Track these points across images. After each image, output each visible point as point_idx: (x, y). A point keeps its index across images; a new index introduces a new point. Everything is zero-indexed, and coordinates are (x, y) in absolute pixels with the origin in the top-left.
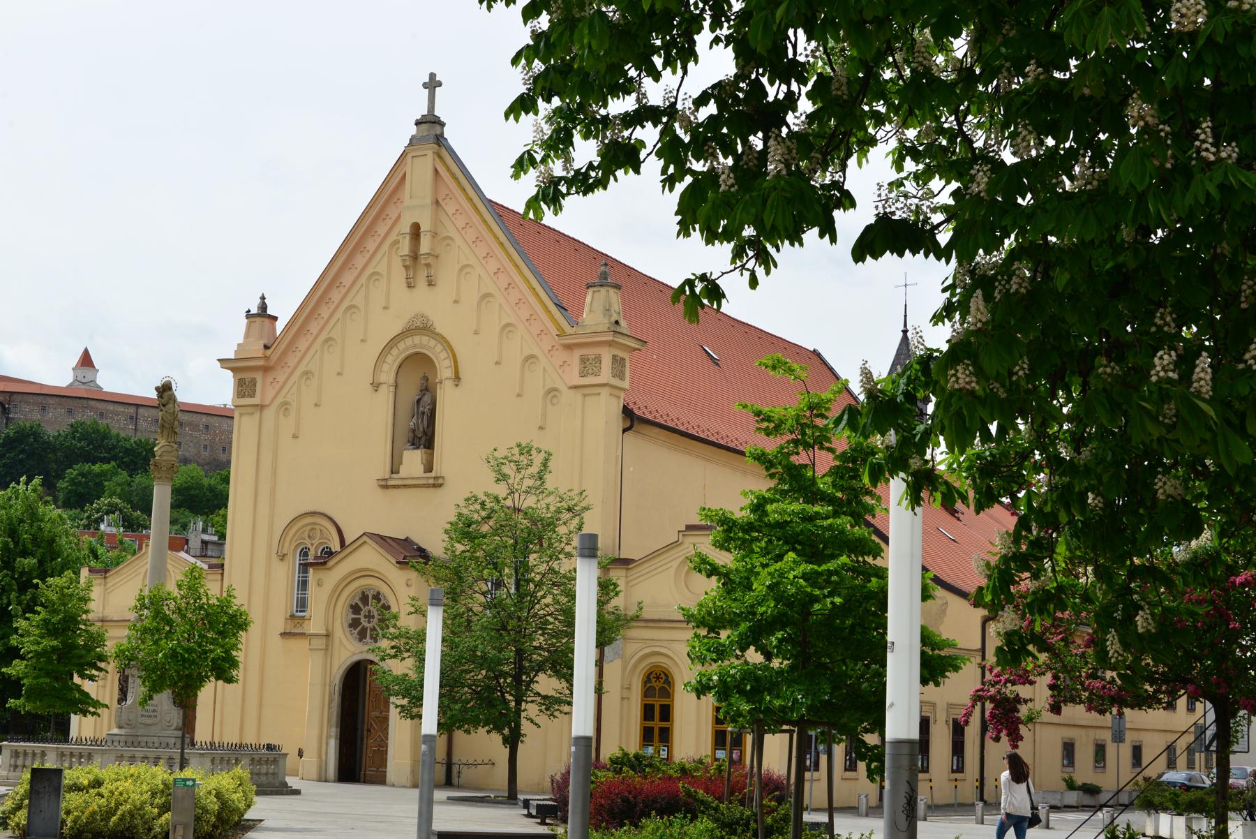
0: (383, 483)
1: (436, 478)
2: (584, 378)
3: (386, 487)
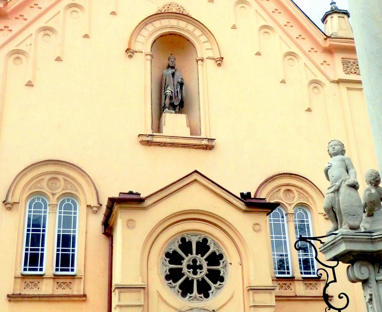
0: (149, 139)
1: (209, 140)
2: (348, 75)
3: (149, 143)
